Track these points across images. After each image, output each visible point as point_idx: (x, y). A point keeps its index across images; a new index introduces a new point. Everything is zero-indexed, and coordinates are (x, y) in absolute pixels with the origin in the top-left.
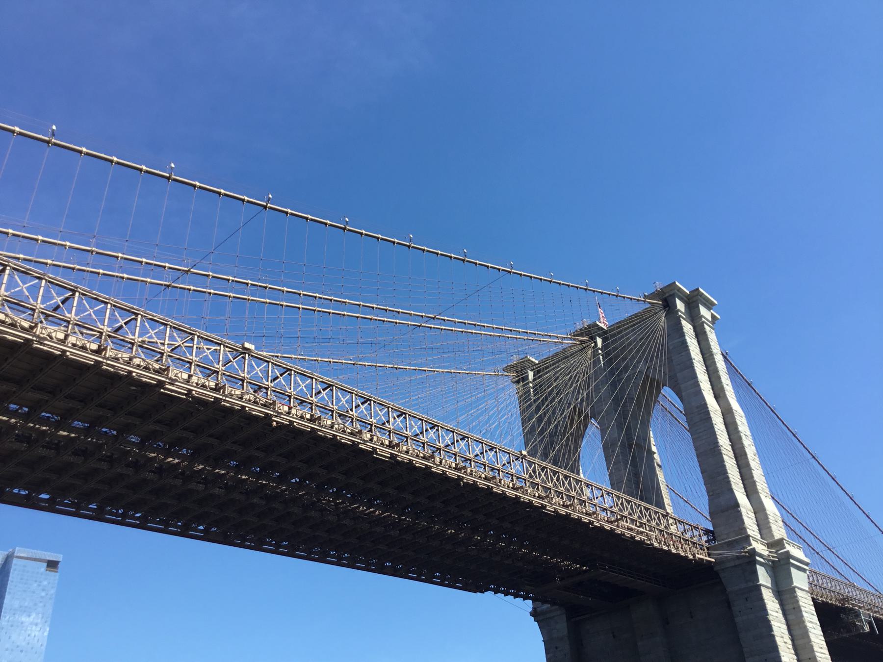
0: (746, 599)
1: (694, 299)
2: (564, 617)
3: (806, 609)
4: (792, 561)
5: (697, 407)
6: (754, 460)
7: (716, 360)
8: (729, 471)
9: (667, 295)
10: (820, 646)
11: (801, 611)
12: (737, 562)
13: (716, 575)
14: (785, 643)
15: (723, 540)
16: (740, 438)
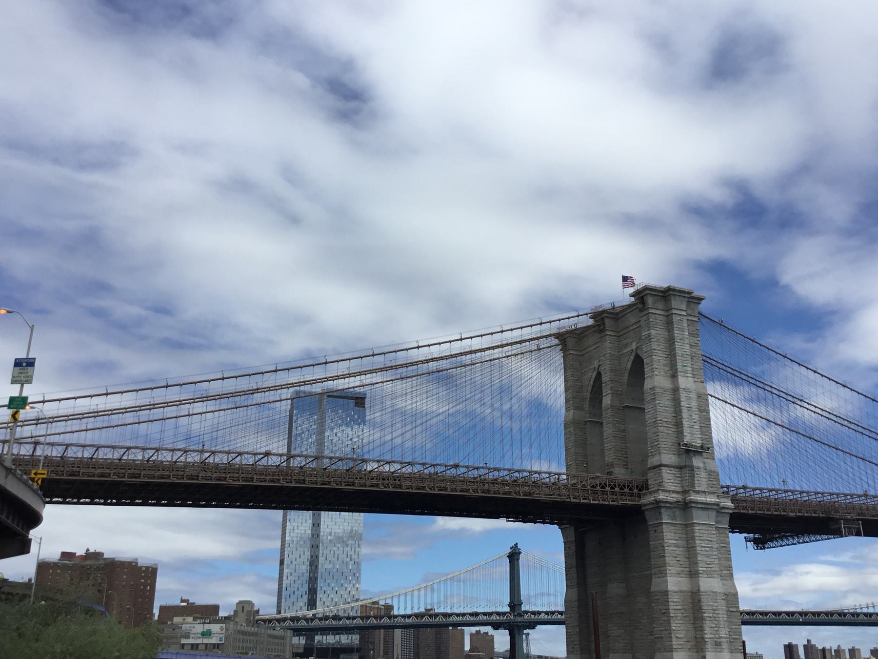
0: (655, 531)
1: (668, 294)
3: (701, 538)
4: (693, 505)
5: (650, 389)
6: (691, 427)
7: (677, 346)
8: (661, 439)
9: (643, 294)
10: (708, 563)
11: (695, 540)
12: (652, 506)
13: (642, 512)
14: (677, 561)
15: (652, 488)
16: (681, 411)
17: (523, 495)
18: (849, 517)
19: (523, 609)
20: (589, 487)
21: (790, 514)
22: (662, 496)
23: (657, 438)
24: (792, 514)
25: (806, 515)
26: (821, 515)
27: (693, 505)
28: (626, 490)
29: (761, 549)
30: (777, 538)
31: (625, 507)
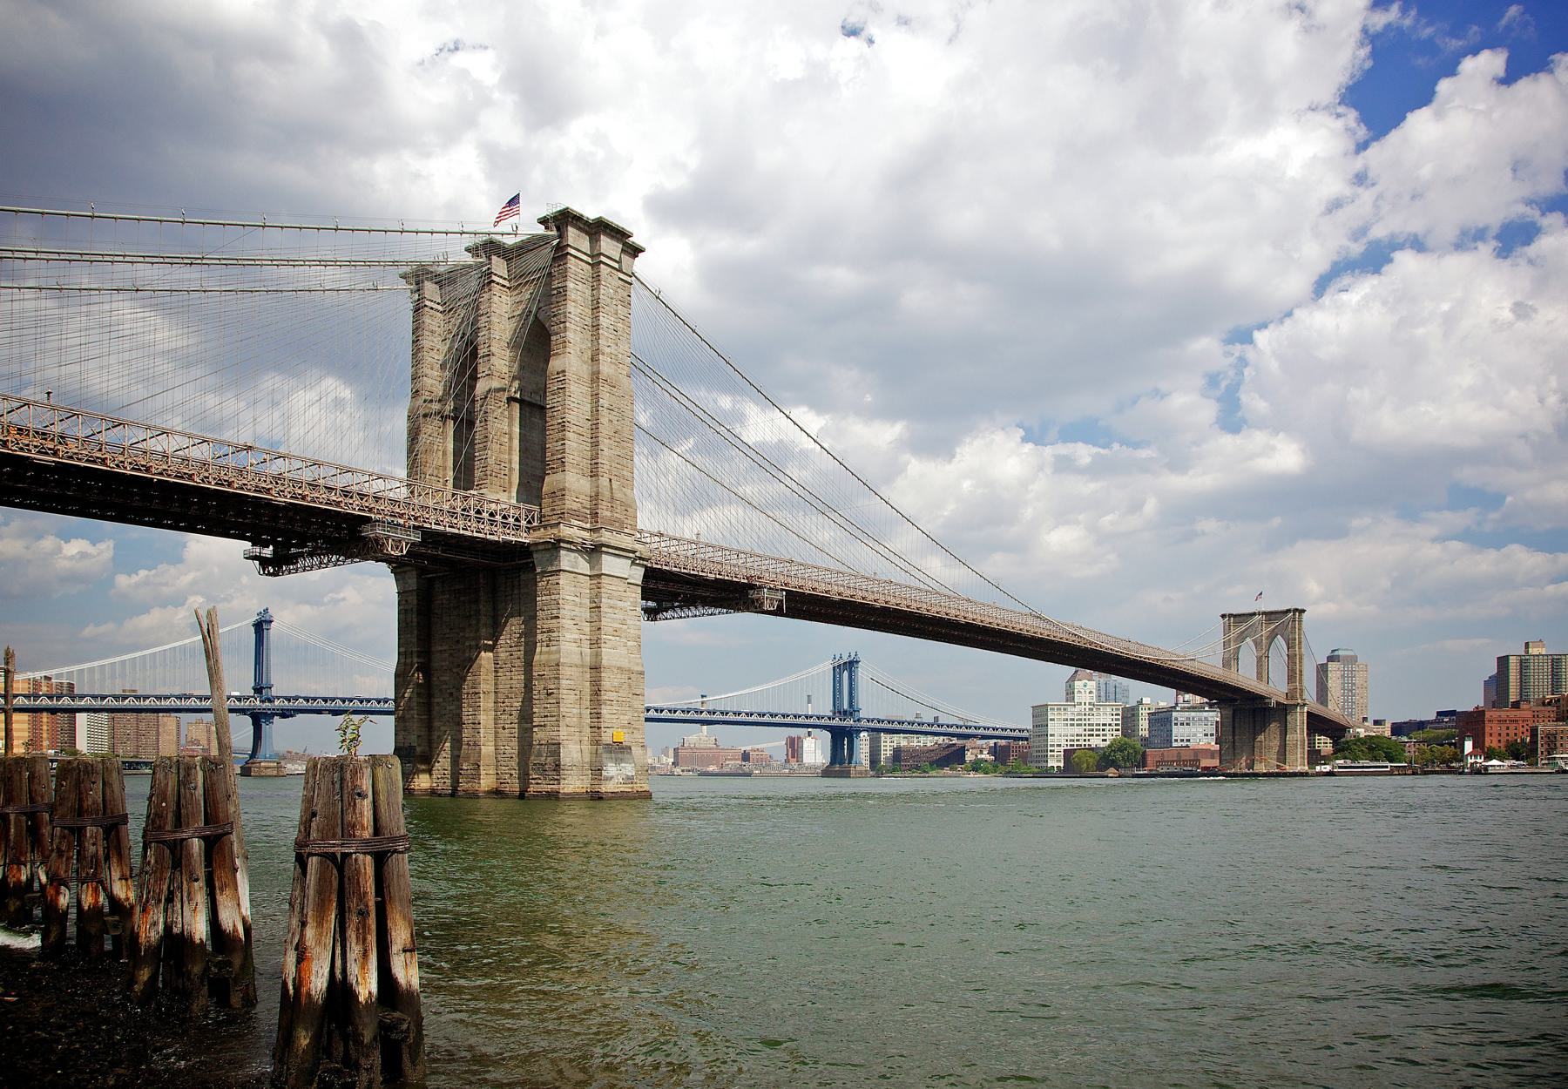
2: (414, 573)
4: (603, 549)
17: (359, 509)
18: (772, 586)
19: (274, 692)
20: (459, 510)
21: (709, 575)
22: (566, 531)
23: (561, 448)
24: (712, 576)
25: (726, 578)
26: (742, 581)
27: (603, 549)
28: (511, 520)
29: (652, 620)
30: (676, 607)
31: (507, 544)
